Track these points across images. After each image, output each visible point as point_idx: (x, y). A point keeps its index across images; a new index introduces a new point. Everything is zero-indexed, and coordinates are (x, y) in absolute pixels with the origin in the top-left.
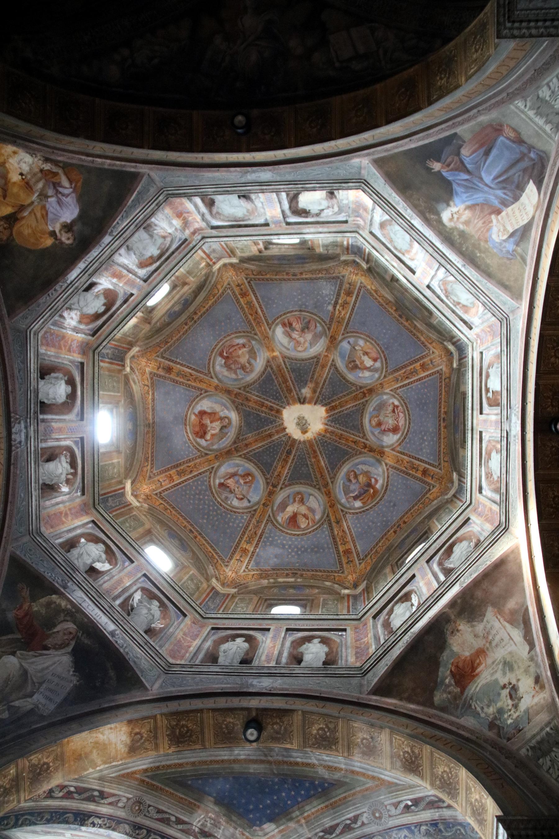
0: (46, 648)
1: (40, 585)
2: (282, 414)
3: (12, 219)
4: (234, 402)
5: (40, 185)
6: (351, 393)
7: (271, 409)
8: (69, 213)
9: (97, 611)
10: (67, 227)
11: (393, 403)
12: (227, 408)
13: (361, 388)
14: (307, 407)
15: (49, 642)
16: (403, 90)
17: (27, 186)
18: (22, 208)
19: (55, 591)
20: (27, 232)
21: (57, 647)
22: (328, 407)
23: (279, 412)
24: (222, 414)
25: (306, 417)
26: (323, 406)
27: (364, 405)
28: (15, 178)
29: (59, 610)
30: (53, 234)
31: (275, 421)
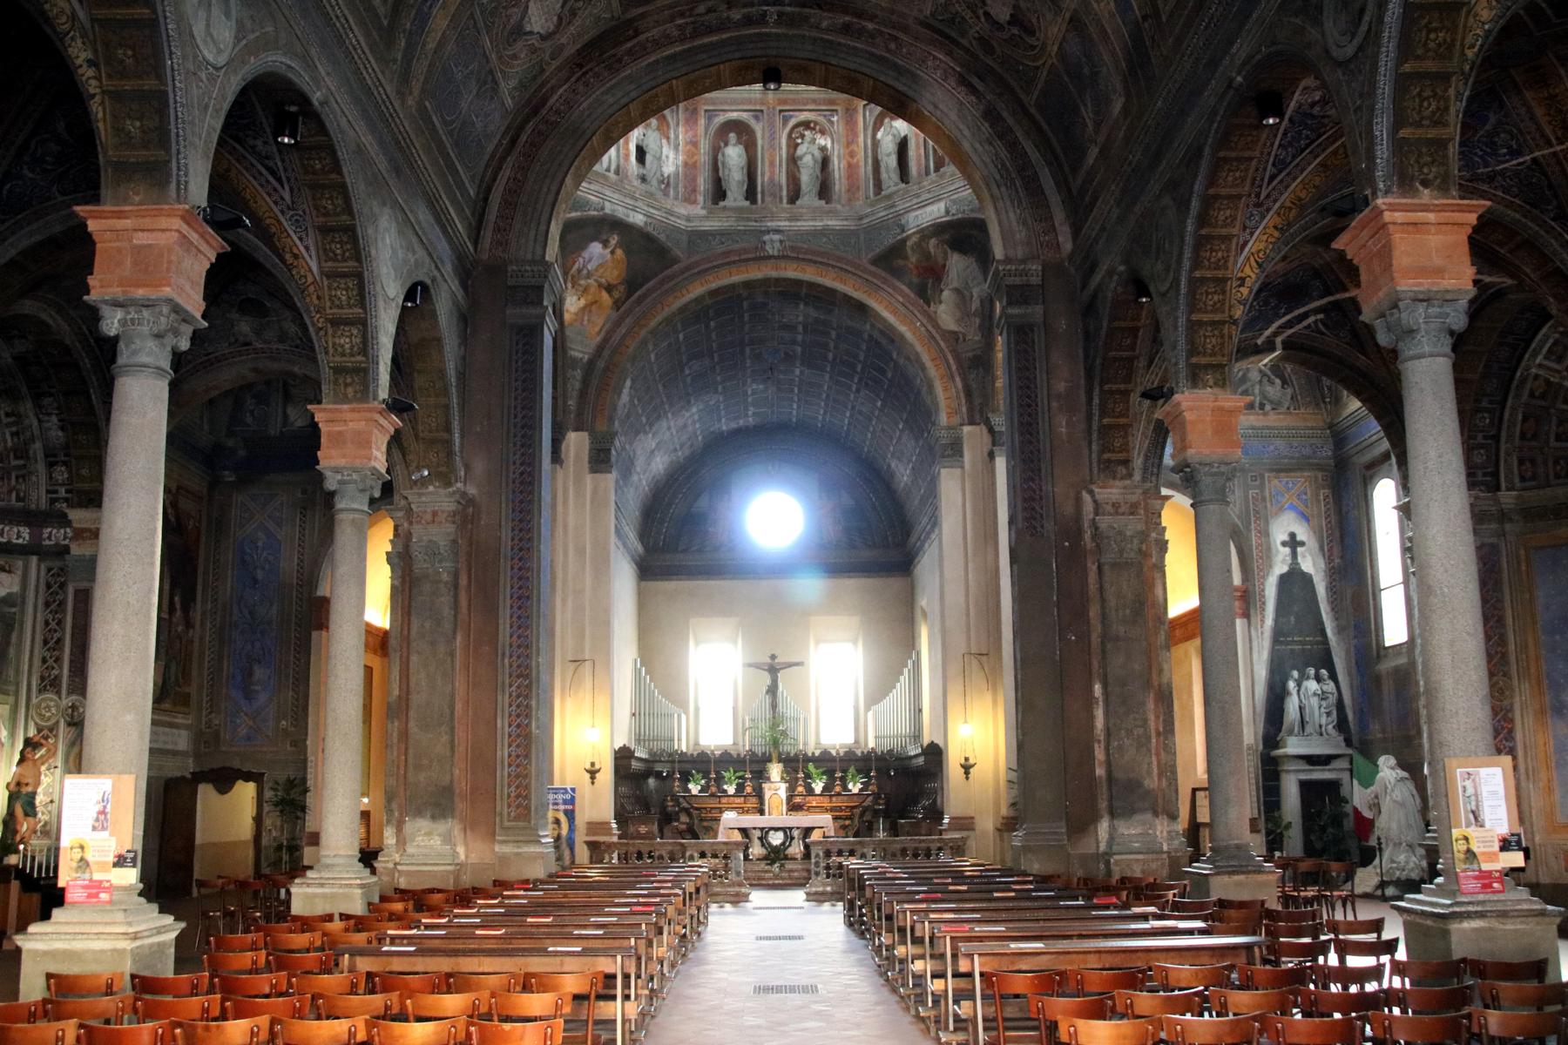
0: (944, 266)
1: (897, 250)
3: (609, 289)
5: (582, 282)
8: (596, 248)
9: (929, 209)
10: (605, 244)
15: (940, 261)
17: (586, 290)
18: (600, 285)
19: (904, 241)
20: (616, 273)
21: (946, 259)
28: (582, 302)
29: (918, 245)
30: (612, 252)
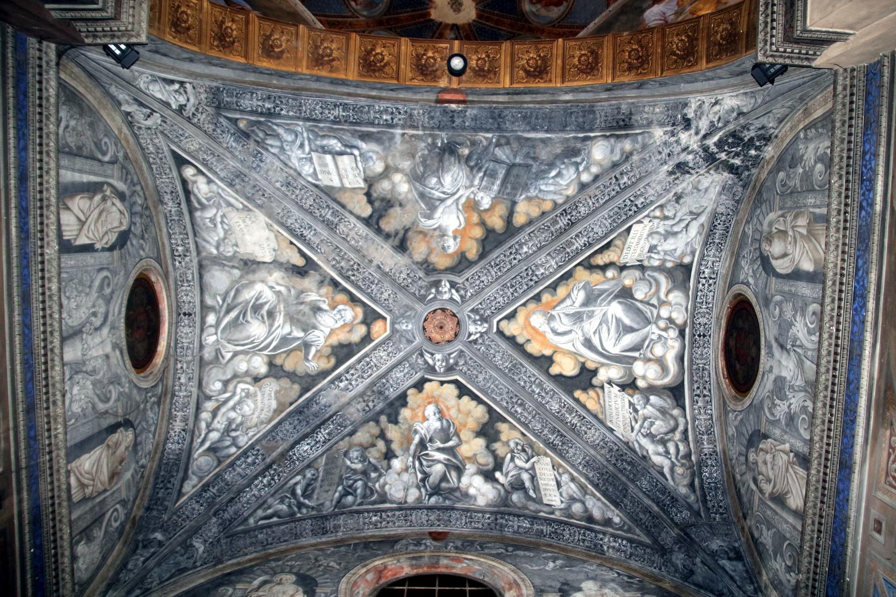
2: (477, 14)
4: (527, 21)
6: (401, 27)
7: (488, 19)
11: (357, 5)
12: (533, 13)
13: (391, 29)
14: (450, 21)
16: (276, 50)
22: (428, 18)
23: (479, 16)
24: (539, 6)
25: (451, 11)
26: (432, 20)
27: (387, 12)
31: (485, 7)
